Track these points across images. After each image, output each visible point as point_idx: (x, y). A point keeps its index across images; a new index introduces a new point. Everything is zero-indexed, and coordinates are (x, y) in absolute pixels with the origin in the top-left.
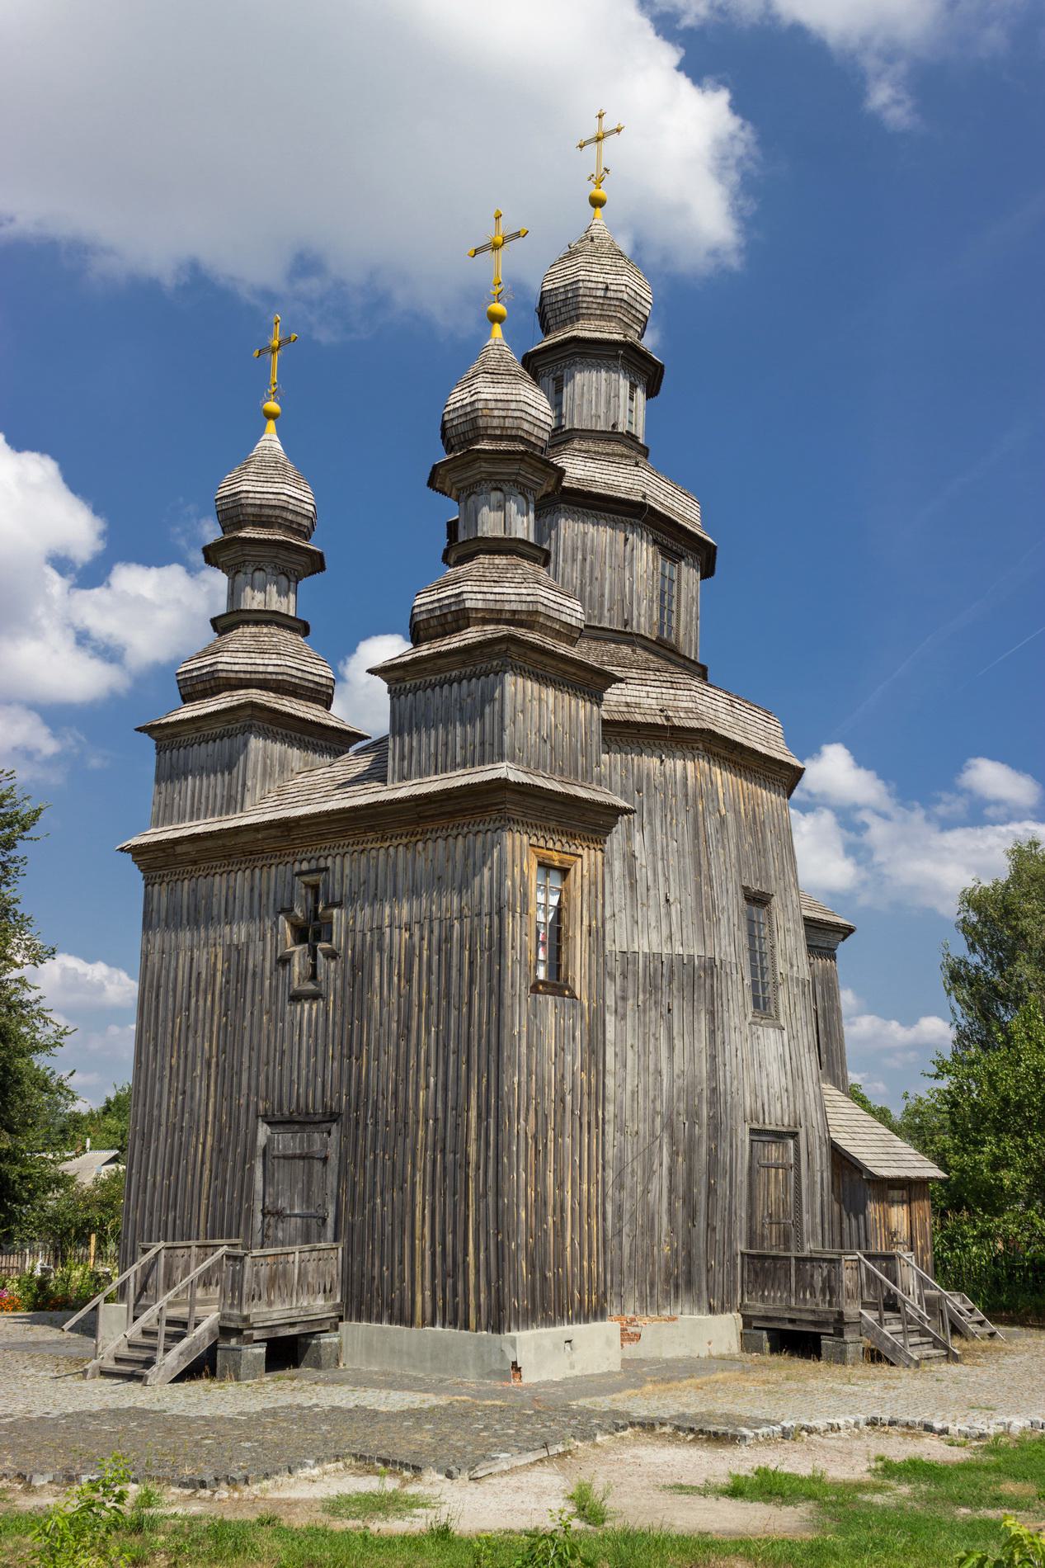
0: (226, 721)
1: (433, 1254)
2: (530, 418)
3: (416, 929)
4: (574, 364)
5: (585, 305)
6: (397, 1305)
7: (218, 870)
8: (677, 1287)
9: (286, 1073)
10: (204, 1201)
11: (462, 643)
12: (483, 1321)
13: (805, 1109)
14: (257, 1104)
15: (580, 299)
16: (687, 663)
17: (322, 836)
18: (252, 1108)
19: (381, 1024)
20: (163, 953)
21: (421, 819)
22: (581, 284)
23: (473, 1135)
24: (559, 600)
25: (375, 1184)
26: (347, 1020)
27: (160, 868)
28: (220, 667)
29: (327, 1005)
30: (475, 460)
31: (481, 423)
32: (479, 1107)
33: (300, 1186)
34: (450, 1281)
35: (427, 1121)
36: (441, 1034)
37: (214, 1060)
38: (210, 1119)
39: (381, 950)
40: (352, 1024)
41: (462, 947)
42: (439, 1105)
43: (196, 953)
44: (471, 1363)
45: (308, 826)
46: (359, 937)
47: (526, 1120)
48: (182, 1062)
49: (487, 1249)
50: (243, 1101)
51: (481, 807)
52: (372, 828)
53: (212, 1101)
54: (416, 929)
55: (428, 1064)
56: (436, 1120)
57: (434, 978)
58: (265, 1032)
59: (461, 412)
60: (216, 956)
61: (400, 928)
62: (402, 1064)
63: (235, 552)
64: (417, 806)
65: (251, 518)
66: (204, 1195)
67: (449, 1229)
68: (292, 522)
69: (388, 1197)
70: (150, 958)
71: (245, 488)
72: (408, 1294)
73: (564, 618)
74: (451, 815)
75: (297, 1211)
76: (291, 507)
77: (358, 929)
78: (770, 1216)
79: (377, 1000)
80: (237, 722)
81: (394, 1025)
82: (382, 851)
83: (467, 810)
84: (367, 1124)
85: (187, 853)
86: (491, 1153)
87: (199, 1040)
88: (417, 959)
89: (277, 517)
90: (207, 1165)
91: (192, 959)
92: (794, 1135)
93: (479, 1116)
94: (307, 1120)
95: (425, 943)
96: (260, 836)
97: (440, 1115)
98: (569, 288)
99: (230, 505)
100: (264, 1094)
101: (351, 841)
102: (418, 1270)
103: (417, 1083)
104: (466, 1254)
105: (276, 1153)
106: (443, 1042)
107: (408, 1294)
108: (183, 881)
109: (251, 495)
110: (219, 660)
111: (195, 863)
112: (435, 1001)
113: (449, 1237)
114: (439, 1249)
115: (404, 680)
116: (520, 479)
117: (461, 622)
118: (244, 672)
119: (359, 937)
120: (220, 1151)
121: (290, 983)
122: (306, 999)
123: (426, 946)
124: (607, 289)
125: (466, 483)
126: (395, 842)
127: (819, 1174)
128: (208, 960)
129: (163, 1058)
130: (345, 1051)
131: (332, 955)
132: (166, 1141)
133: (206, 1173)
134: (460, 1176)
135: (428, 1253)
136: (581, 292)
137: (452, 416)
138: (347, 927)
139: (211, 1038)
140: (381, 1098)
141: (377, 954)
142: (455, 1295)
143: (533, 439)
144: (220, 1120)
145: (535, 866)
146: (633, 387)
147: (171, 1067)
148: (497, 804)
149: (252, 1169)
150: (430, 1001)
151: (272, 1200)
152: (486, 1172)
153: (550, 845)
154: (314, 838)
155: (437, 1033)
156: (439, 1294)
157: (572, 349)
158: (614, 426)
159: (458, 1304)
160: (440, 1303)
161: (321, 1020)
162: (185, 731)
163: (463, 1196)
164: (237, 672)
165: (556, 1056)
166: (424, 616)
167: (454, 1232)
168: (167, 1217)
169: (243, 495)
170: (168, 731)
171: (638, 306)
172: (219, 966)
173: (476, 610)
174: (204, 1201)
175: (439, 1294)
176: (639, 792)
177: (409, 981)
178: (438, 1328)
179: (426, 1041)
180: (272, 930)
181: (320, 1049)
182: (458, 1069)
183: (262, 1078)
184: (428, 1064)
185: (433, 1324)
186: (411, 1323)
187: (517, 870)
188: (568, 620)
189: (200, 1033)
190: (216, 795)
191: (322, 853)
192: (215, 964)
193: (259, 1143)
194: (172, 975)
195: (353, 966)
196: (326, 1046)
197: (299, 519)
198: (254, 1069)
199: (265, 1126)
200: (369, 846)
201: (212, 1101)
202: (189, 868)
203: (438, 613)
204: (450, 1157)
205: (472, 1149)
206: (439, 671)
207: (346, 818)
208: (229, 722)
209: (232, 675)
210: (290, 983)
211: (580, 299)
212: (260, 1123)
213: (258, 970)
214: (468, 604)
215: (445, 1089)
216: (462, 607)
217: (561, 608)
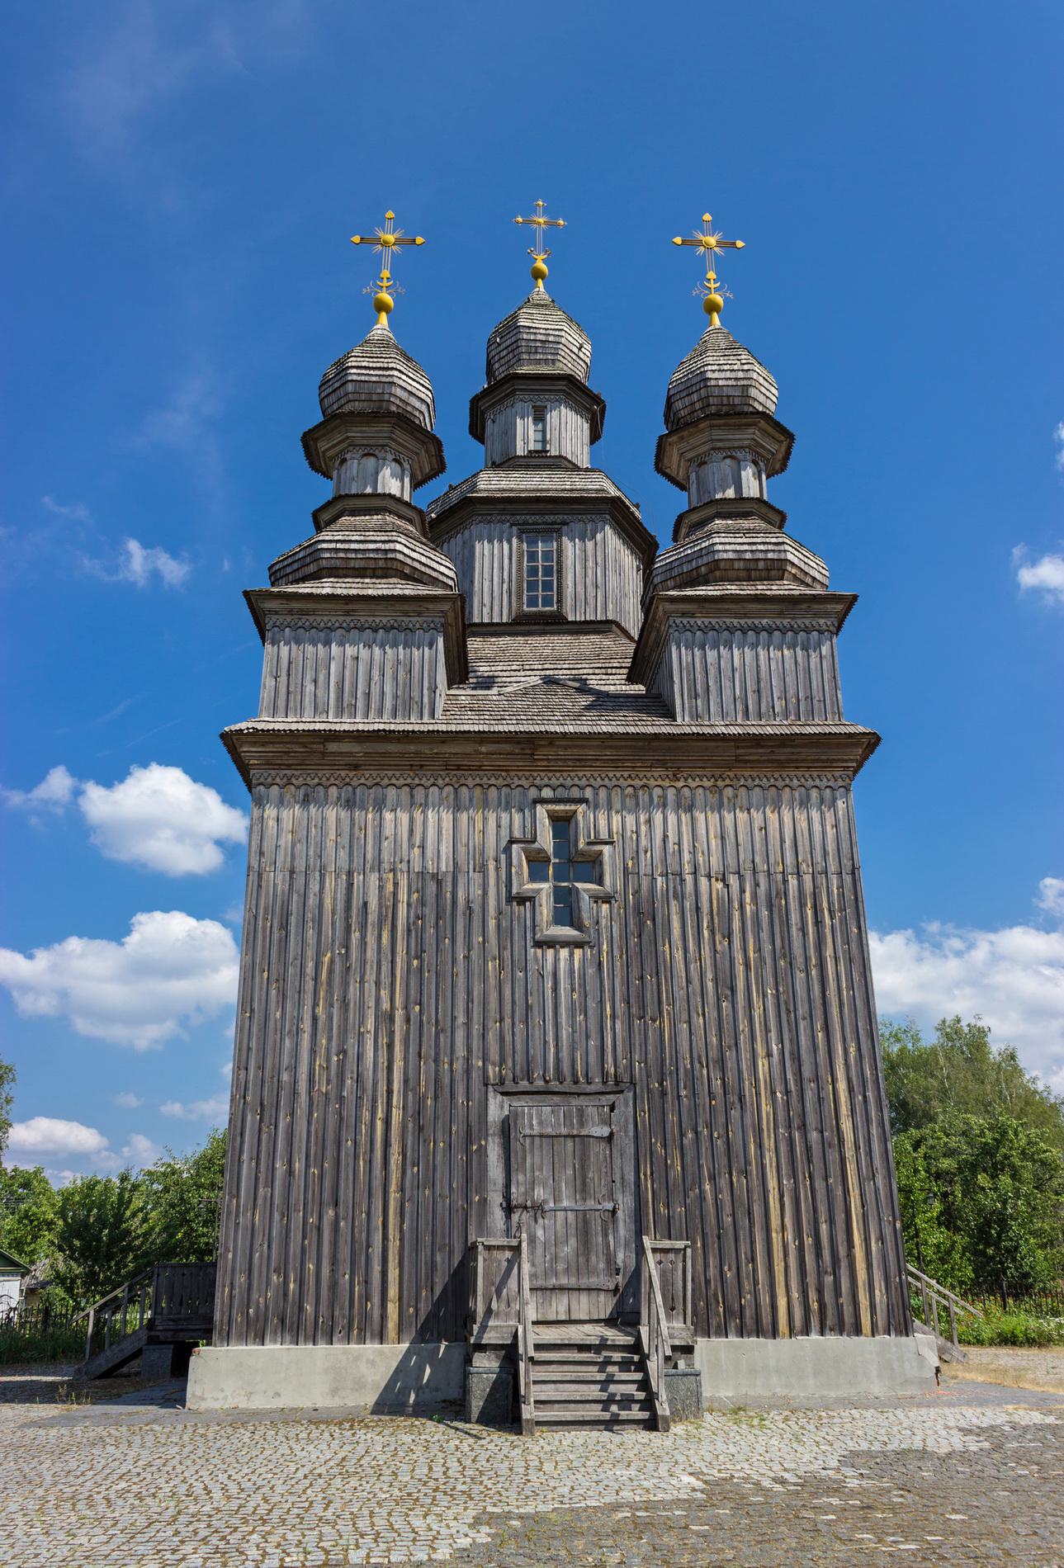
0: (401, 611)
1: (801, 1249)
3: (733, 880)
4: (559, 402)
5: (563, 354)
6: (748, 1313)
7: (394, 781)
9: (537, 1033)
10: (394, 1196)
11: (786, 593)
12: (881, 1323)
14: (485, 1070)
15: (561, 346)
17: (582, 763)
18: (476, 1075)
19: (688, 981)
20: (292, 872)
21: (740, 762)
22: (563, 333)
23: (844, 1110)
25: (700, 1167)
26: (635, 971)
27: (289, 767)
28: (398, 547)
29: (600, 953)
30: (749, 425)
31: (753, 392)
32: (849, 1081)
33: (570, 1172)
34: (829, 1279)
35: (773, 1093)
36: (783, 998)
37: (399, 1014)
38: (397, 1086)
39: (680, 897)
40: (642, 978)
41: (802, 905)
42: (790, 1076)
43: (358, 879)
44: (874, 1373)
45: (566, 748)
46: (645, 882)
48: (335, 1011)
49: (881, 1238)
50: (459, 1066)
51: (823, 761)
52: (662, 764)
53: (398, 1065)
54: (733, 880)
55: (767, 1030)
56: (787, 1092)
57: (765, 935)
58: (492, 982)
59: (728, 375)
60: (396, 884)
61: (709, 877)
62: (726, 1030)
63: (377, 432)
64: (738, 748)
65: (398, 402)
66: (393, 1187)
67: (823, 1217)
69: (723, 1182)
70: (264, 876)
71: (399, 367)
72: (765, 1299)
74: (781, 765)
75: (565, 1204)
77: (642, 872)
79: (679, 955)
80: (419, 614)
81: (710, 985)
82: (671, 793)
83: (804, 761)
84: (679, 1096)
85: (350, 754)
86: (874, 1131)
87: (370, 987)
88: (736, 915)
89: (421, 412)
90: (395, 1148)
91: (350, 885)
93: (850, 1089)
94: (574, 1089)
95: (748, 895)
96: (483, 749)
97: (792, 1086)
98: (551, 332)
99: (374, 379)
100: (497, 1058)
101: (626, 774)
102: (779, 1268)
103: (754, 1050)
104: (850, 1244)
105: (528, 1132)
106: (785, 1008)
107: (765, 1299)
108: (327, 788)
109: (404, 377)
110: (399, 539)
111: (356, 767)
112: (769, 961)
113: (824, 1228)
114: (808, 1241)
115: (693, 616)
117: (773, 573)
118: (420, 562)
119: (645, 882)
120: (420, 1129)
121: (534, 926)
122: (562, 947)
123: (748, 900)
124: (580, 349)
125: (727, 444)
126: (693, 784)
128: (381, 888)
129: (300, 1004)
130: (634, 1010)
131: (608, 899)
132: (310, 1114)
133: (395, 1158)
134: (833, 1156)
135: (792, 1247)
136: (563, 340)
137: (716, 375)
138: (625, 868)
139: (393, 984)
140: (697, 1065)
141: (674, 906)
142: (837, 1293)
144: (416, 1090)
147: (315, 1019)
148: (846, 761)
149: (483, 1152)
150: (762, 959)
151: (522, 1189)
152: (870, 1153)
154: (570, 763)
155: (777, 996)
156: (813, 1295)
157: (562, 386)
159: (842, 1304)
160: (815, 1306)
161: (591, 971)
162: (324, 610)
163: (839, 1179)
164: (413, 559)
166: (731, 556)
167: (831, 1221)
168: (320, 1218)
169: (396, 373)
170: (295, 605)
172: (403, 896)
173: (793, 564)
174: (394, 1196)
175: (813, 1295)
177: (729, 936)
178: (815, 1336)
179: (763, 1006)
180: (497, 860)
181: (592, 1005)
182: (813, 1038)
183: (492, 1037)
184: (767, 1030)
185: (806, 1331)
186: (775, 1334)
189: (371, 976)
190: (383, 693)
191: (576, 781)
192: (395, 894)
193: (490, 1119)
194: (312, 901)
195: (638, 912)
196: (601, 1002)
198: (476, 1027)
199: (499, 1097)
200: (652, 783)
201: (398, 1065)
202: (343, 773)
203: (748, 556)
204: (814, 1136)
205: (846, 1125)
206: (745, 616)
207: (625, 747)
208: (406, 614)
209: (409, 561)
210: (534, 926)
211: (561, 346)
212: (491, 1094)
213: (476, 907)
214: (790, 557)
215: (797, 1058)
216: (782, 556)
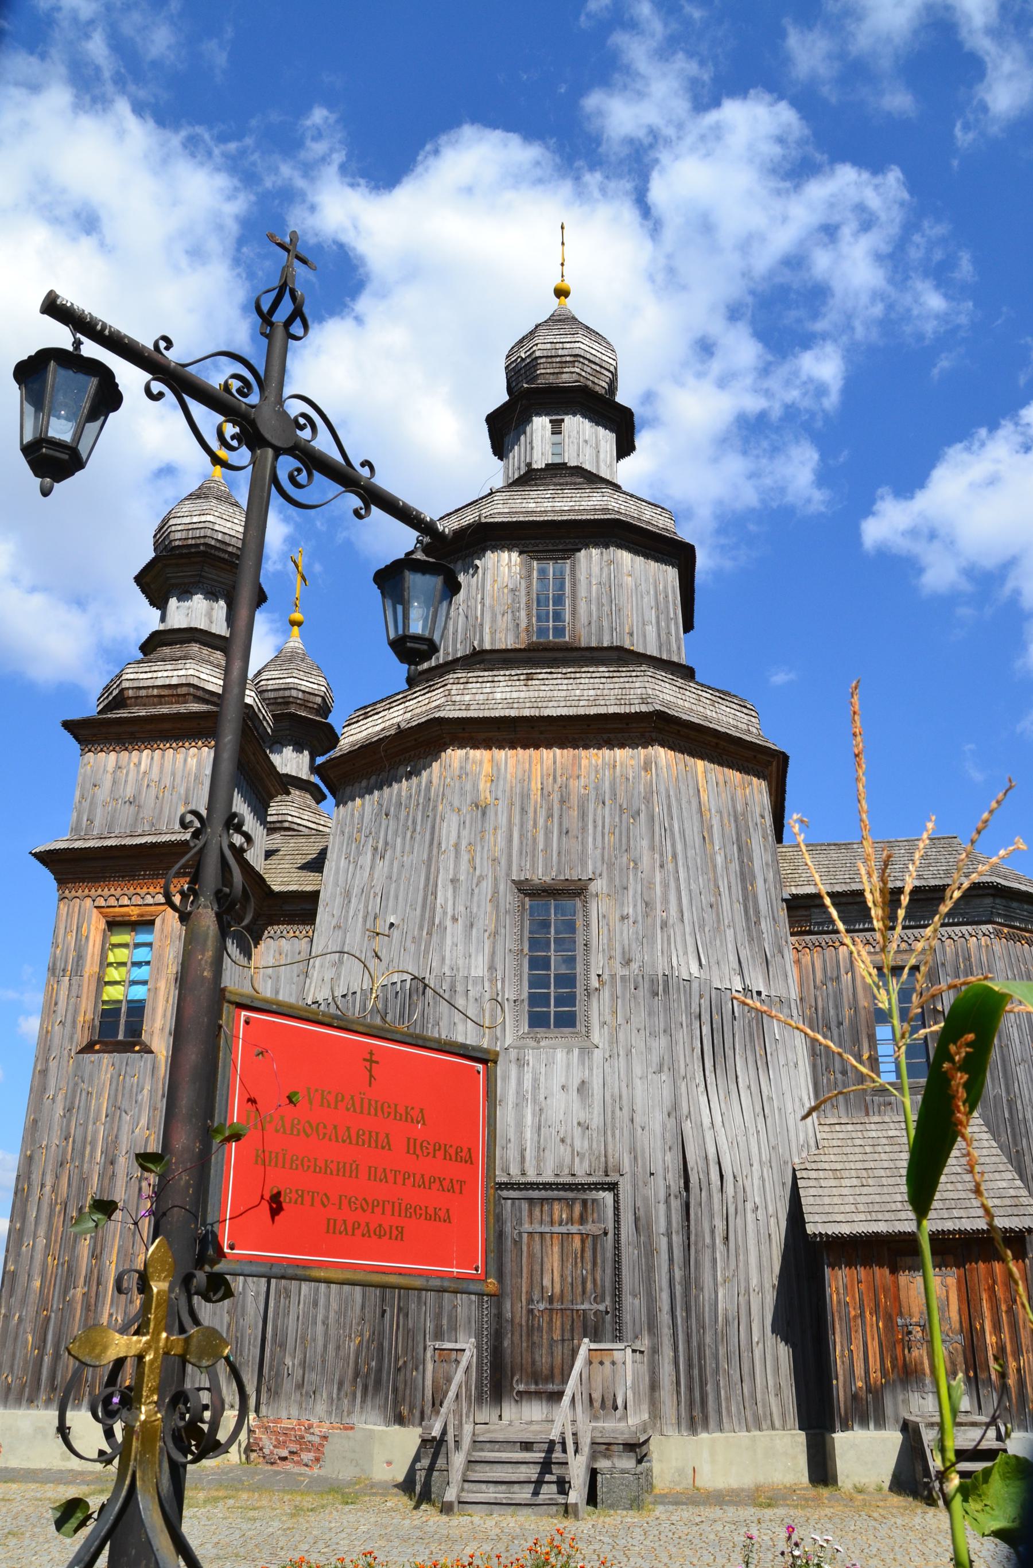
2: (179, 528)
8: (365, 1388)
13: (633, 1150)
16: (587, 654)
24: (153, 669)
47: (54, 1189)
68: (276, 698)
73: (159, 682)
76: (269, 688)
78: (551, 1300)
92: (613, 1187)
116: (173, 581)
127: (664, 1240)
143: (190, 542)
145: (102, 925)
153: (125, 901)
158: (529, 465)
165: (107, 1116)
171: (560, 352)
176: (387, 815)
187: (71, 939)
188: (167, 682)
197: (281, 693)
217: (155, 675)
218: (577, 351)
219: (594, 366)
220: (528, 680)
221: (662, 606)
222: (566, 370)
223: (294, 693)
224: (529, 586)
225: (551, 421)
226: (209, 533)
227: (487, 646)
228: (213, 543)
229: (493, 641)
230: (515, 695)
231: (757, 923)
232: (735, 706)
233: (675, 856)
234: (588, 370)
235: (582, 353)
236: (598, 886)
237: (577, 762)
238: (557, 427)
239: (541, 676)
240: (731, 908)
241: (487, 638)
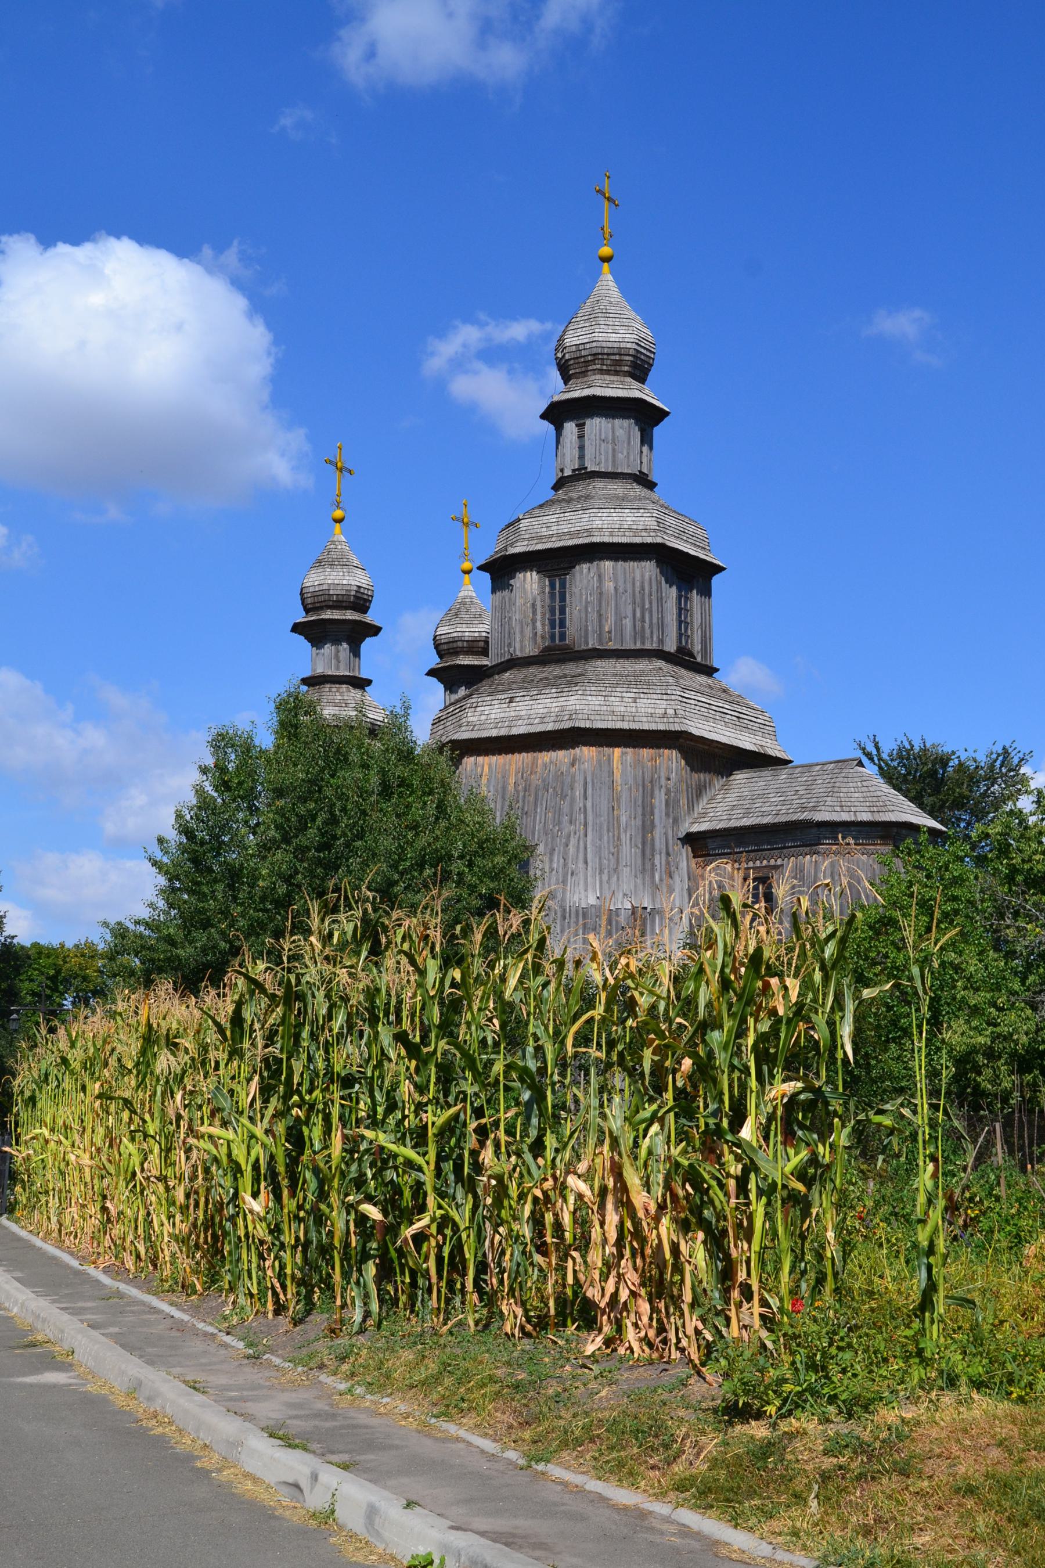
146: (581, 426)
218: (594, 351)
219: (613, 357)
220: (510, 702)
221: (638, 600)
222: (590, 368)
223: (460, 644)
224: (543, 601)
225: (577, 425)
226: (327, 598)
227: (519, 654)
228: (331, 603)
229: (522, 648)
230: (502, 715)
231: (652, 860)
232: (655, 696)
233: (585, 825)
234: (609, 362)
235: (599, 351)
236: (541, 849)
237: (534, 763)
238: (581, 426)
239: (518, 699)
240: (629, 852)
241: (518, 646)
